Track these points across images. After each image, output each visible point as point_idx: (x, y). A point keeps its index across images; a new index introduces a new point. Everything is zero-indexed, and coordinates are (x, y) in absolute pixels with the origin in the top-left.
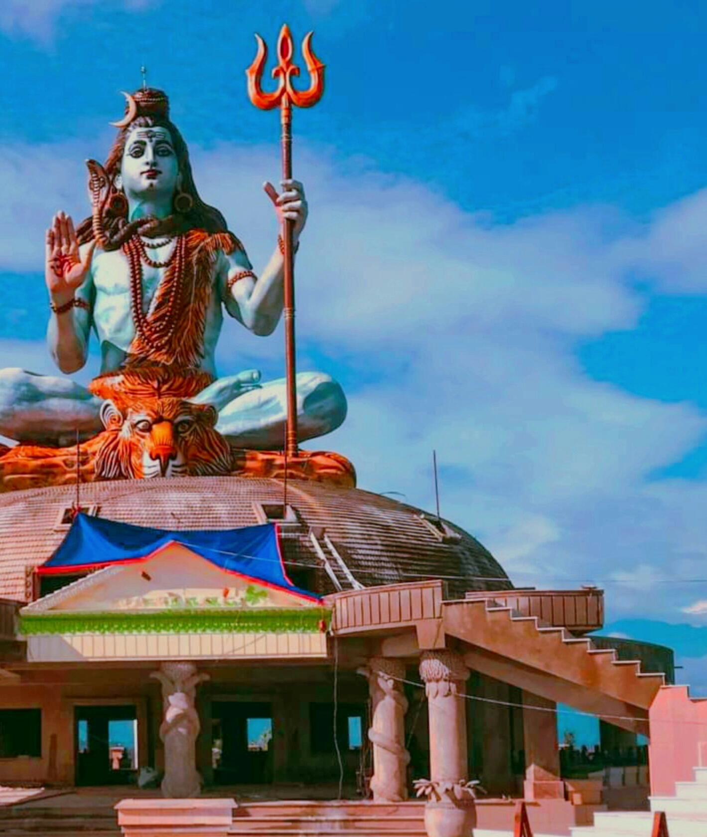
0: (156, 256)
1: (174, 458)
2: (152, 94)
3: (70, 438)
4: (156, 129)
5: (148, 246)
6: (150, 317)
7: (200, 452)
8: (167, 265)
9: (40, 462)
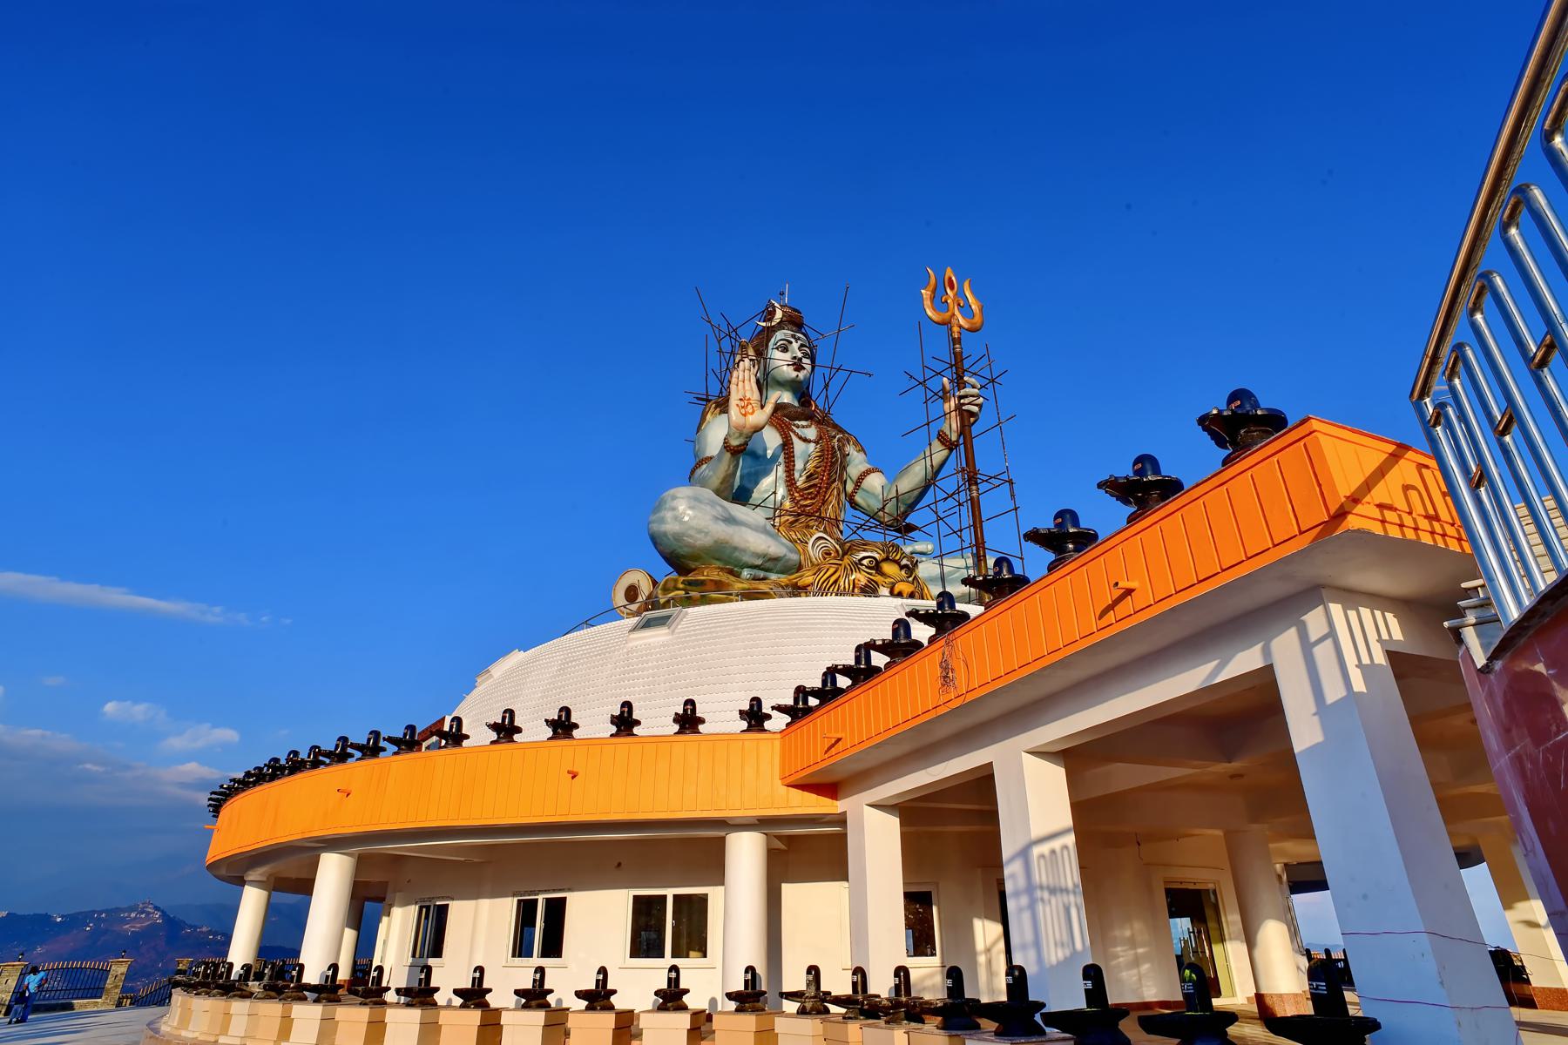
3: (754, 572)
6: (800, 483)
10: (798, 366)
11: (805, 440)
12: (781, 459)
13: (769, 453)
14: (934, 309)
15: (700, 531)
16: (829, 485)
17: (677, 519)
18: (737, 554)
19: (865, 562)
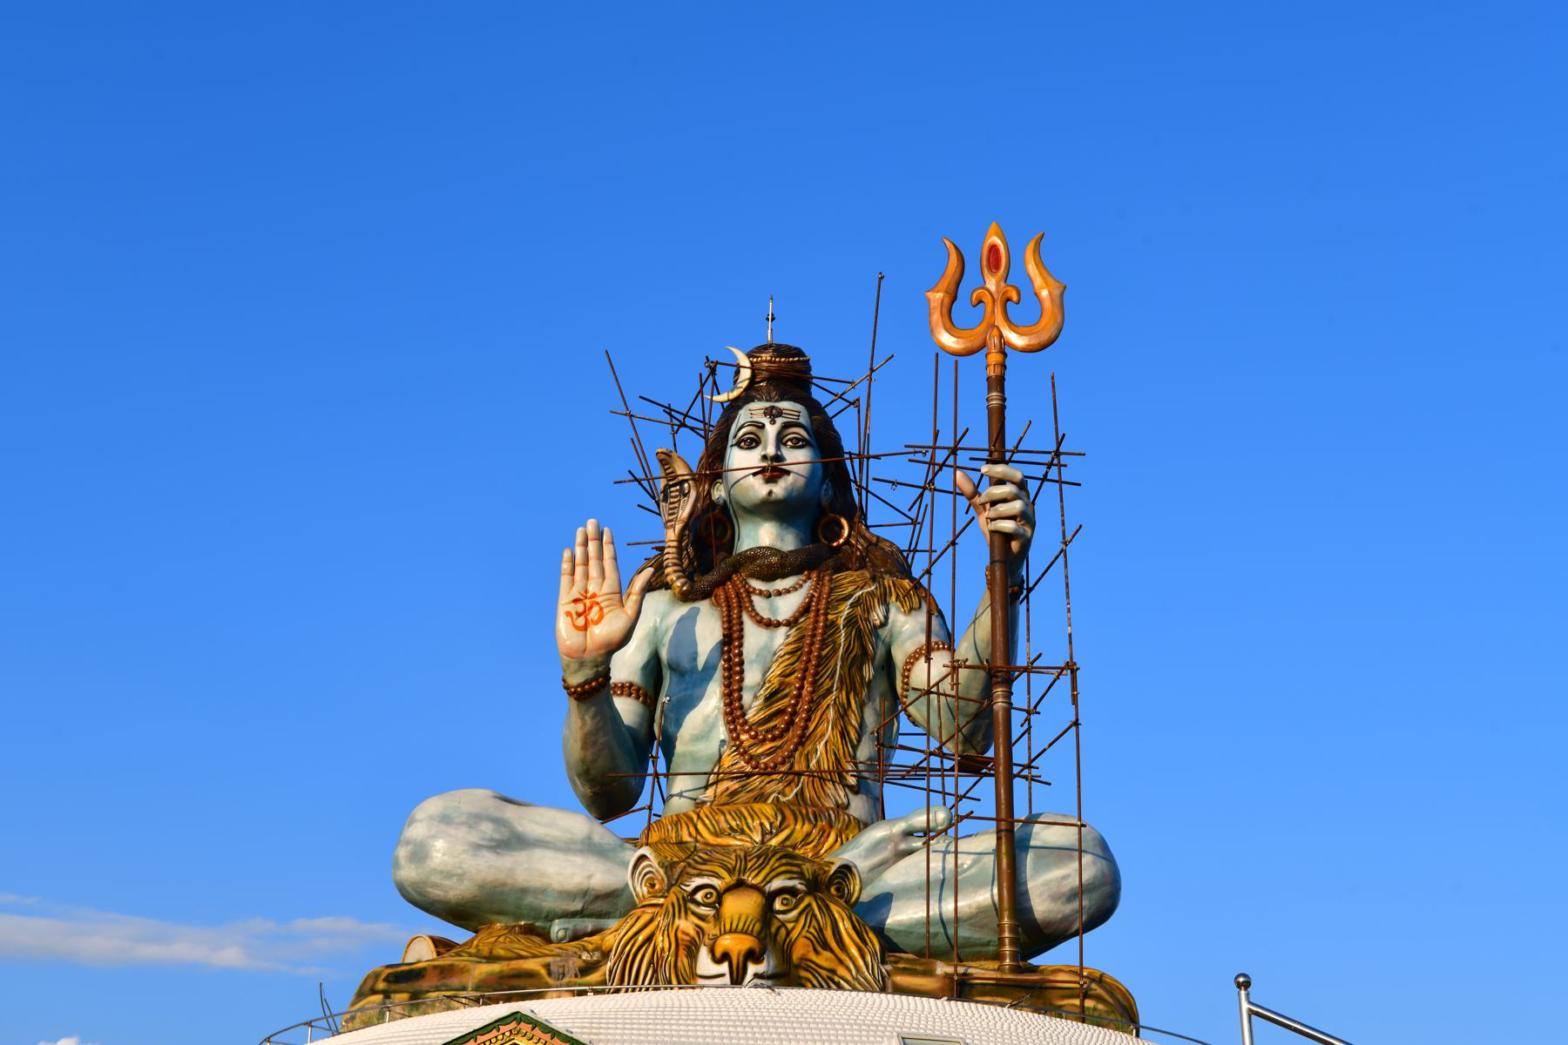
0: (773, 609)
1: (758, 961)
2: (780, 350)
5: (761, 593)
6: (752, 716)
8: (790, 624)
9: (496, 967)
10: (773, 470)
11: (770, 624)
12: (719, 675)
14: (951, 327)
15: (449, 875)
16: (814, 704)
17: (420, 854)
18: (529, 900)
19: (699, 896)
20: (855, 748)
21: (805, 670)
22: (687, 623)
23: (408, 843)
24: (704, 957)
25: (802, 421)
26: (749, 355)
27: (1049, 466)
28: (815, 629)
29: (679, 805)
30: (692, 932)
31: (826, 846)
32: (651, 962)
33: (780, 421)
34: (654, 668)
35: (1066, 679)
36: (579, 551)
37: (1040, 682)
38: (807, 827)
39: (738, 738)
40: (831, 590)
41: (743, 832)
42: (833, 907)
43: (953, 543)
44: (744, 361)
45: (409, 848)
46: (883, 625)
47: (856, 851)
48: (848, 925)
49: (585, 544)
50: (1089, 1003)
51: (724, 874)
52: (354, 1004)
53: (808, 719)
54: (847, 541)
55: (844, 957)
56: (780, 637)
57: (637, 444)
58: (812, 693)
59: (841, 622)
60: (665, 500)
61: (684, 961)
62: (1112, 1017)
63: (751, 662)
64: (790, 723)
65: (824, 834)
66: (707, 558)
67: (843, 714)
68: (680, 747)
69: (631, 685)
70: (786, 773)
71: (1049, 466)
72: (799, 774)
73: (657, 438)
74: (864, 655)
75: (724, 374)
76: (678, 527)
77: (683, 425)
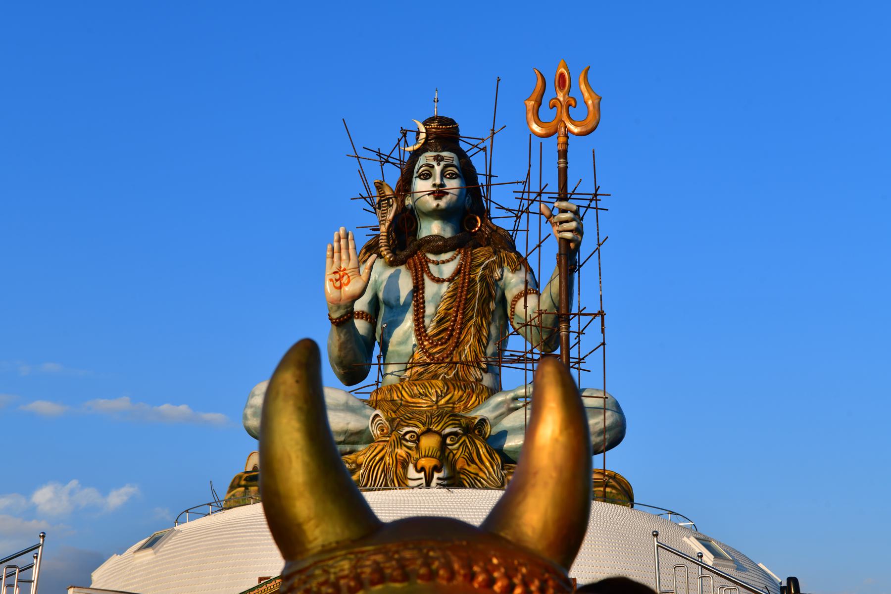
0: (440, 272)
1: (439, 471)
4: (444, 154)
5: (433, 262)
6: (430, 331)
7: (469, 465)
8: (450, 280)
10: (439, 192)
11: (439, 281)
12: (411, 309)
13: (402, 300)
14: (539, 122)
16: (464, 324)
19: (407, 437)
20: (485, 348)
21: (459, 306)
22: (394, 278)
23: (252, 407)
24: (411, 468)
25: (455, 163)
26: (424, 124)
27: (591, 200)
28: (463, 283)
29: (391, 379)
30: (404, 456)
31: (471, 402)
32: (383, 470)
33: (442, 163)
34: (375, 302)
35: (599, 318)
36: (336, 245)
37: (585, 320)
38: (460, 393)
39: (422, 344)
40: (472, 260)
41: (426, 396)
42: (477, 442)
43: (539, 246)
44: (423, 129)
45: (253, 410)
46: (500, 279)
47: (487, 409)
48: (484, 450)
49: (339, 241)
50: (608, 490)
51: (420, 425)
52: (229, 492)
53: (460, 333)
54: (480, 229)
55: (482, 467)
56: (445, 288)
57: (362, 173)
58: (462, 319)
59: (477, 279)
60: (379, 208)
61: (400, 470)
62: (620, 497)
63: (429, 302)
64: (451, 336)
65: (470, 396)
66: (402, 242)
67: (479, 330)
68: (390, 348)
69: (363, 312)
70: (449, 363)
71: (591, 200)
72: (456, 363)
73: (374, 173)
74: (490, 297)
75: (411, 136)
76: (387, 224)
77: (387, 161)
